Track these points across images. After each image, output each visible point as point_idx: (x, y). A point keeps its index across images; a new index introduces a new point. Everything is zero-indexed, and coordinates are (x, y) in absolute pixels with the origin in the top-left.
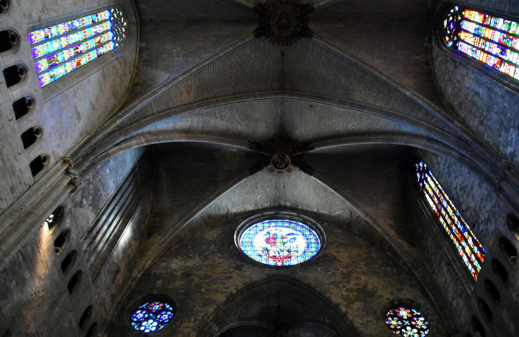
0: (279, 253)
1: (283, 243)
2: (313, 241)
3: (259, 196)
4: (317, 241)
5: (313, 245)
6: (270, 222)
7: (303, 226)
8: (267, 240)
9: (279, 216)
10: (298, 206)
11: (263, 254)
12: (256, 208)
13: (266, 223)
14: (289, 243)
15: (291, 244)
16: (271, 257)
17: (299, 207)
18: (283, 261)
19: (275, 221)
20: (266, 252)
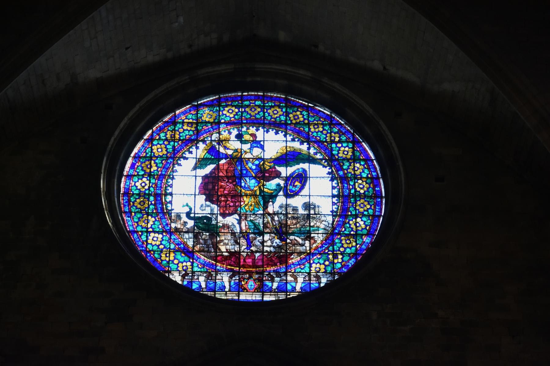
0: (250, 244)
1: (264, 197)
2: (361, 187)
3: (181, 19)
4: (375, 186)
5: (363, 206)
6: (219, 101)
7: (332, 123)
8: (210, 187)
9: (249, 79)
10: (316, 46)
11: (197, 248)
12: (170, 55)
13: (204, 105)
14: (281, 200)
15: (292, 201)
16: (224, 260)
17: (321, 48)
18: (262, 273)
19: (234, 99)
20: (206, 235)
